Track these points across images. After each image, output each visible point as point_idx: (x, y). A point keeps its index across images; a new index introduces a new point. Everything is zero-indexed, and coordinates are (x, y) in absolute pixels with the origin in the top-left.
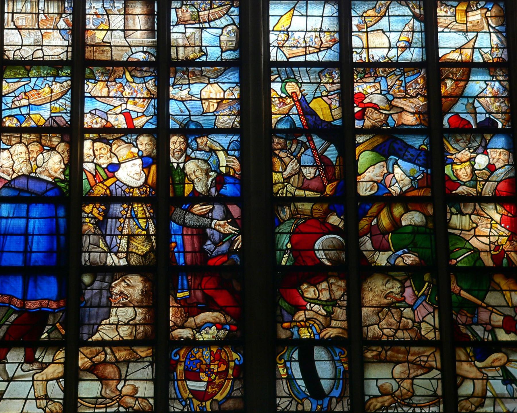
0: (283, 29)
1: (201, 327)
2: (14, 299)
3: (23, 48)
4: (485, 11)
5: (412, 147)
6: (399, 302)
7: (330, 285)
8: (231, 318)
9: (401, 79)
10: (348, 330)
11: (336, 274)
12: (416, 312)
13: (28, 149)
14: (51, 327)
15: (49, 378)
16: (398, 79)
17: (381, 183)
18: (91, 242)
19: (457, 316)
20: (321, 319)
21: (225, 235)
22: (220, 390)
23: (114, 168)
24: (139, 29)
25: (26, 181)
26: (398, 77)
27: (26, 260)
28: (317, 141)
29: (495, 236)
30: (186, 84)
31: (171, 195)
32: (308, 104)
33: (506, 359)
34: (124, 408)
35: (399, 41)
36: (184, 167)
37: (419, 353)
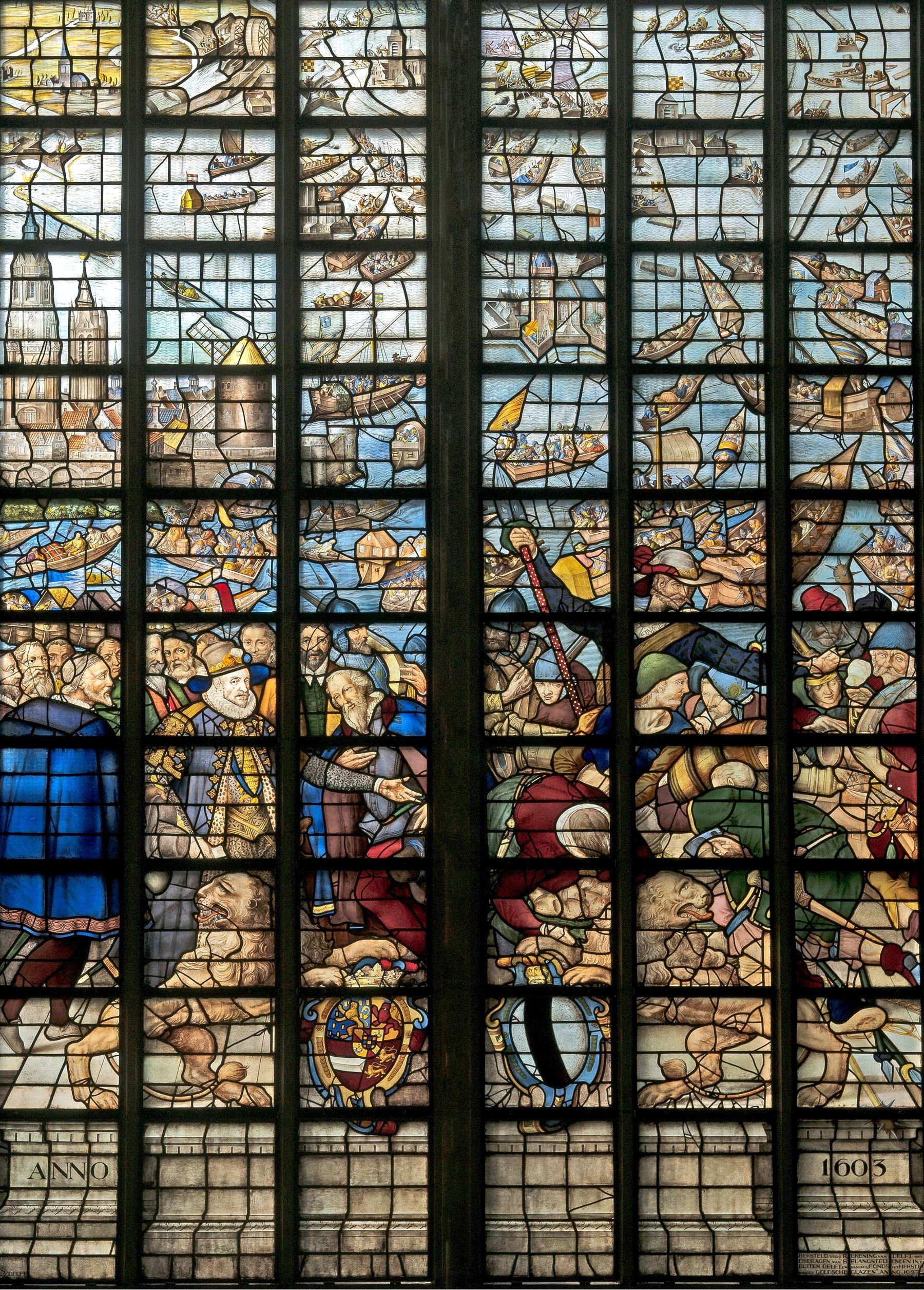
0: (505, 427)
1: (354, 964)
2: (29, 916)
3: (35, 465)
4: (876, 393)
5: (734, 645)
6: (702, 921)
7: (582, 893)
8: (409, 948)
9: (718, 521)
10: (614, 970)
11: (593, 872)
12: (731, 938)
13: (46, 651)
14: (93, 964)
15: (94, 1050)
16: (714, 521)
17: (677, 711)
18: (161, 817)
19: (802, 945)
20: (565, 951)
21: (397, 805)
22: (387, 1072)
23: (200, 685)
24: (243, 427)
25: (44, 709)
26: (714, 516)
27: (49, 849)
28: (565, 634)
29: (875, 805)
30: (328, 532)
31: (303, 733)
32: (550, 567)
33: (884, 1019)
34: (223, 1101)
35: (718, 450)
36: (325, 683)
37: (735, 1009)
